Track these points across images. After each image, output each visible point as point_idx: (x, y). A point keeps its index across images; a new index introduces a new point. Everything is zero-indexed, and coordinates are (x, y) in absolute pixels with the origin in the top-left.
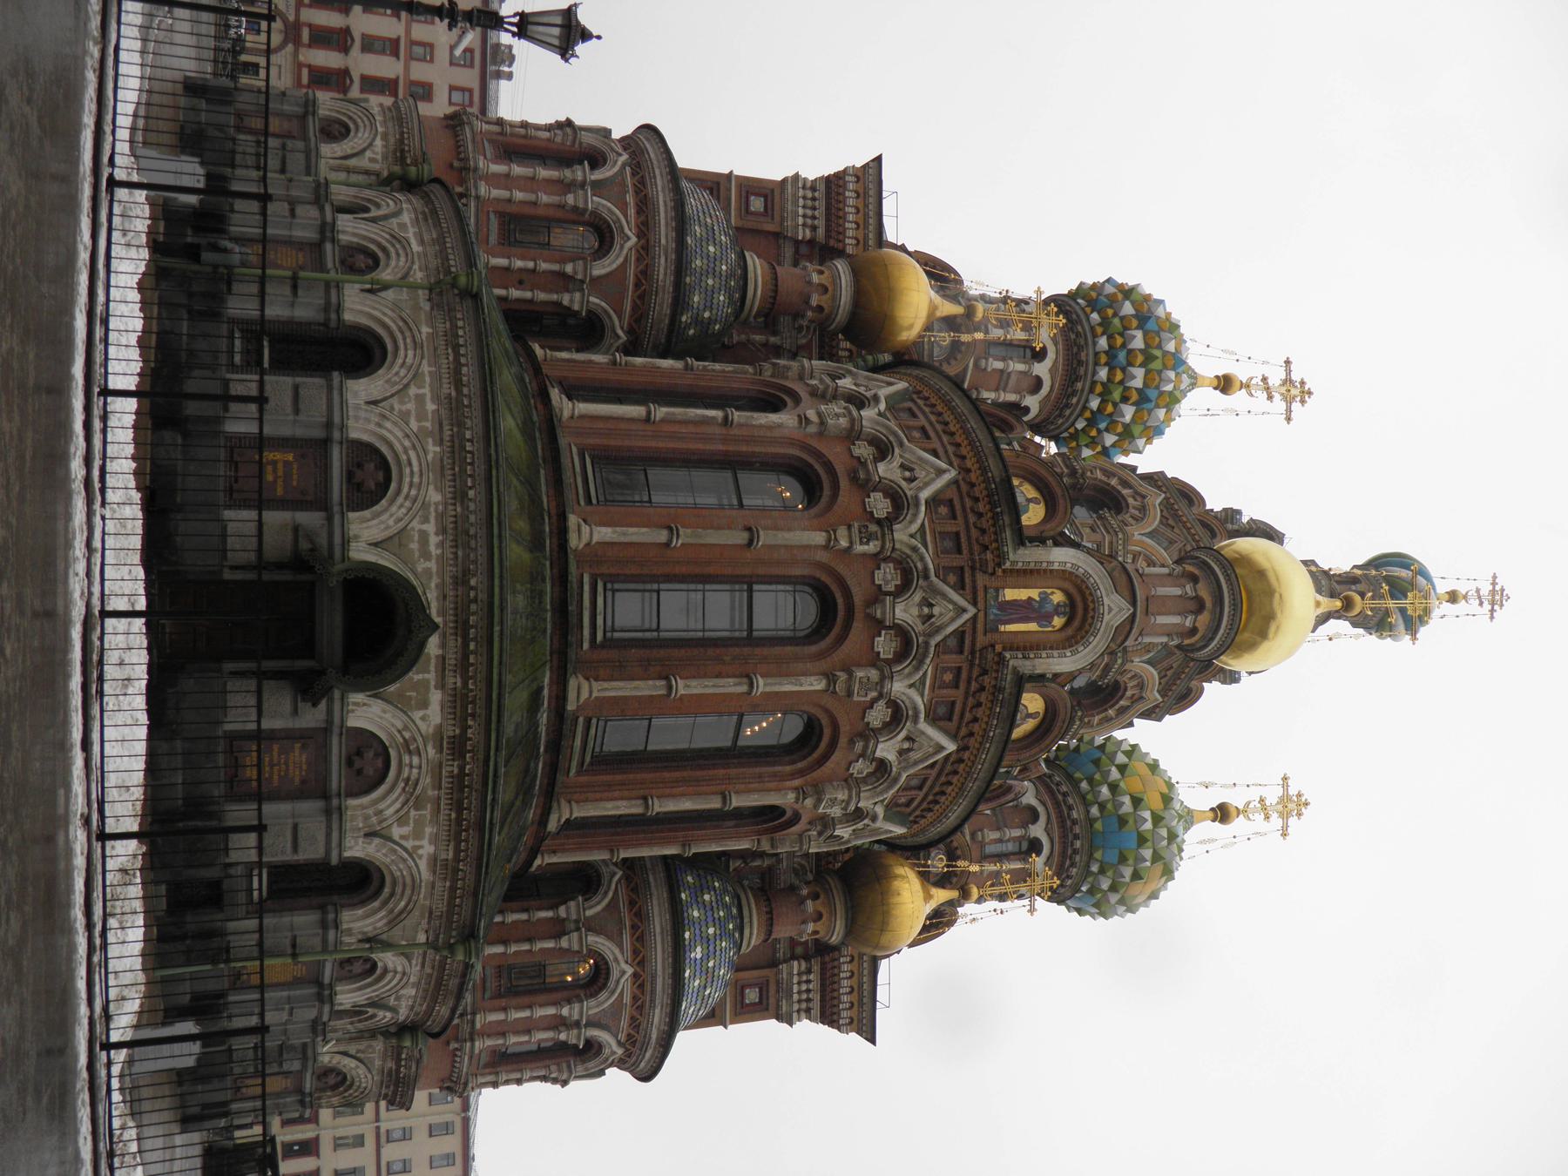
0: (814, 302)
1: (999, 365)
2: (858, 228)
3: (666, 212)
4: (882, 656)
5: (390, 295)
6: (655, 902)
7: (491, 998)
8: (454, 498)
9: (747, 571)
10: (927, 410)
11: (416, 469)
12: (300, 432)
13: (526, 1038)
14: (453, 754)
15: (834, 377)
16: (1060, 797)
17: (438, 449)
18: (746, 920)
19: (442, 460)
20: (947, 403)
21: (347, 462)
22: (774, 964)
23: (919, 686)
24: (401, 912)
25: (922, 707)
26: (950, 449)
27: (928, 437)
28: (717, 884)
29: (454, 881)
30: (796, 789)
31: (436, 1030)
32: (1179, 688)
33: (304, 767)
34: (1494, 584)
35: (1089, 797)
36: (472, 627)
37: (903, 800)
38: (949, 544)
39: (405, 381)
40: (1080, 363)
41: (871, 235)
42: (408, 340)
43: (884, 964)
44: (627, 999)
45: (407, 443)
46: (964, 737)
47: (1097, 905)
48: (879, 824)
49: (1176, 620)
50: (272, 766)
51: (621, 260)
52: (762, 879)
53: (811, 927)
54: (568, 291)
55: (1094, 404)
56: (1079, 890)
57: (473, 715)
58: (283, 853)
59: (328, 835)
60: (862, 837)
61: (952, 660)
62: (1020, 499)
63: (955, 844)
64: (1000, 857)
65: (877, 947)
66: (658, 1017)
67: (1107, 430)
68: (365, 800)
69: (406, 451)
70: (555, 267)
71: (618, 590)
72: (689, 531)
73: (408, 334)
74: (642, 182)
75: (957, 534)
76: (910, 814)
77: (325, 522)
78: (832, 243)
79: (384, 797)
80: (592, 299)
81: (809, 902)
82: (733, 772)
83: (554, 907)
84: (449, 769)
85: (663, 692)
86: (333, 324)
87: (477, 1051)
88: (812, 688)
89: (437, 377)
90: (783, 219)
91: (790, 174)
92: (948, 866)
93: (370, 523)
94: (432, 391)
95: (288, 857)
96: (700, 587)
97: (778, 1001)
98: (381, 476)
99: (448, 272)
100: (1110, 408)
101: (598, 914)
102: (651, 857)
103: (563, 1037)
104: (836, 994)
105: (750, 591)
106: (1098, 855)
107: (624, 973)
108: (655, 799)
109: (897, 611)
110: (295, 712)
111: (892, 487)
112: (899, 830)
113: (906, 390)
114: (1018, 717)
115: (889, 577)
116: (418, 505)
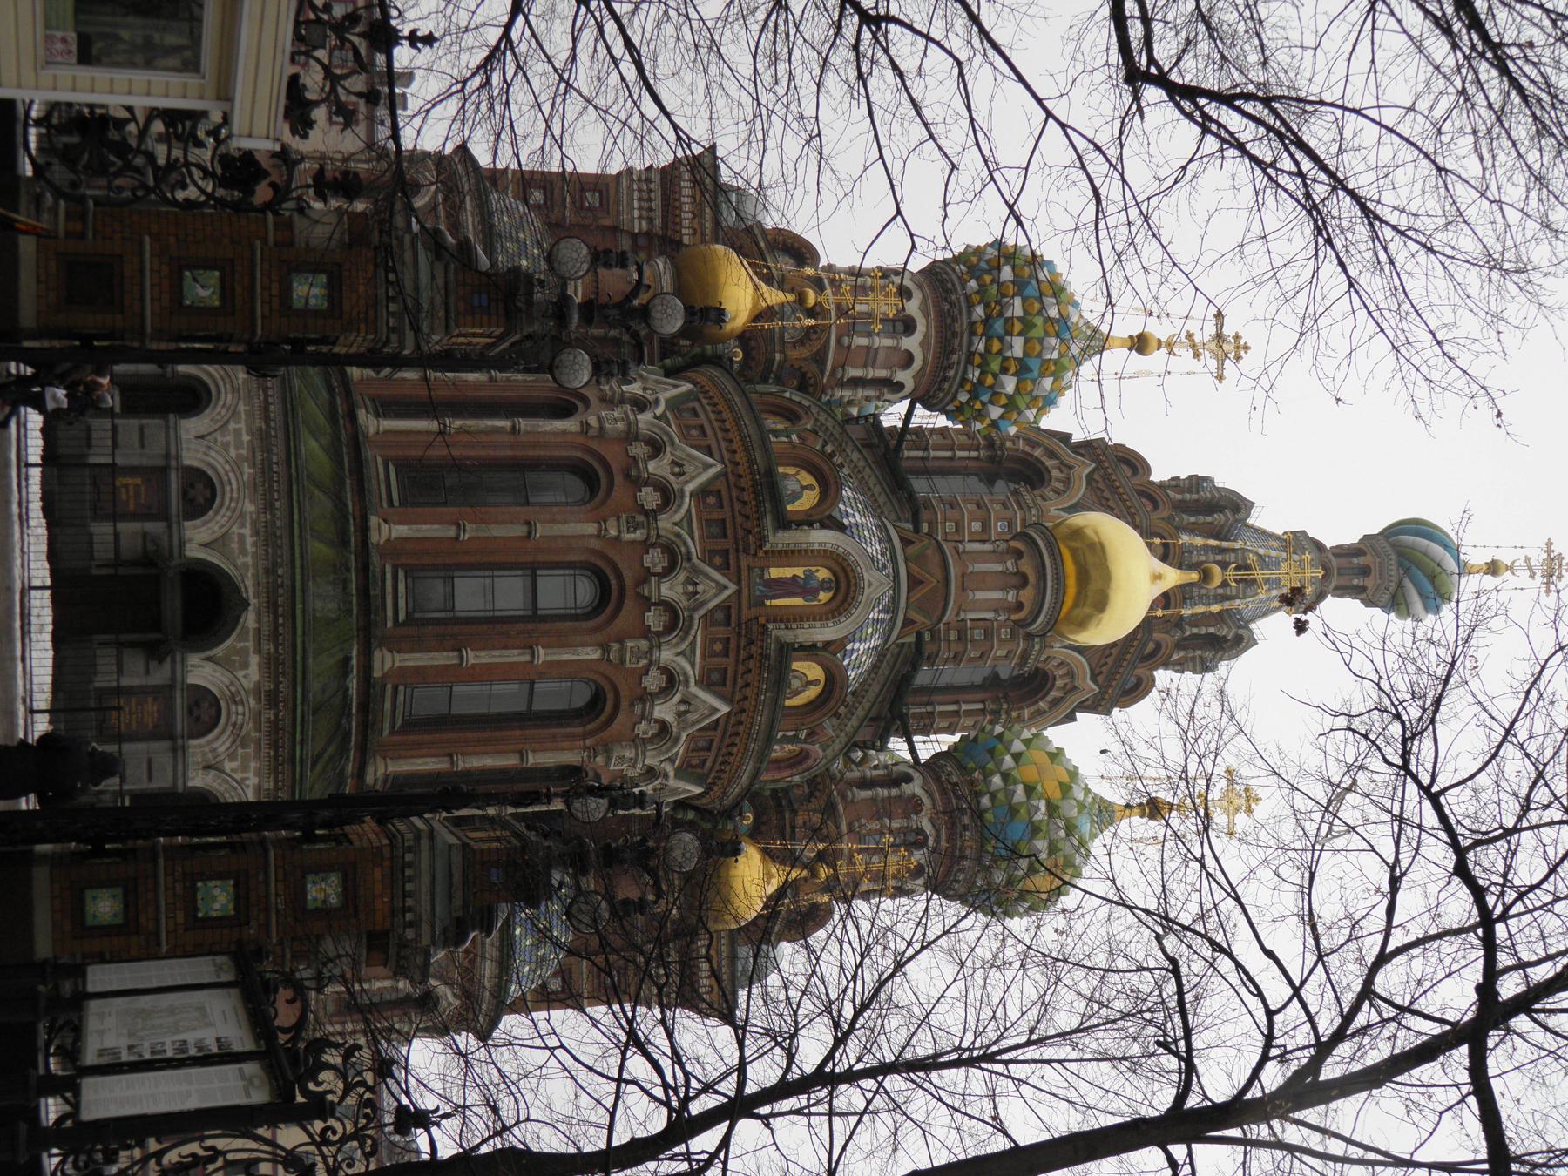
1: (863, 341)
9: (530, 559)
10: (709, 408)
11: (235, 486)
23: (688, 655)
34: (1549, 552)
37: (695, 762)
38: (715, 530)
40: (954, 334)
41: (708, 225)
55: (974, 374)
61: (721, 632)
67: (991, 402)
68: (203, 741)
75: (723, 521)
89: (250, 414)
100: (990, 380)
105: (534, 577)
113: (690, 392)
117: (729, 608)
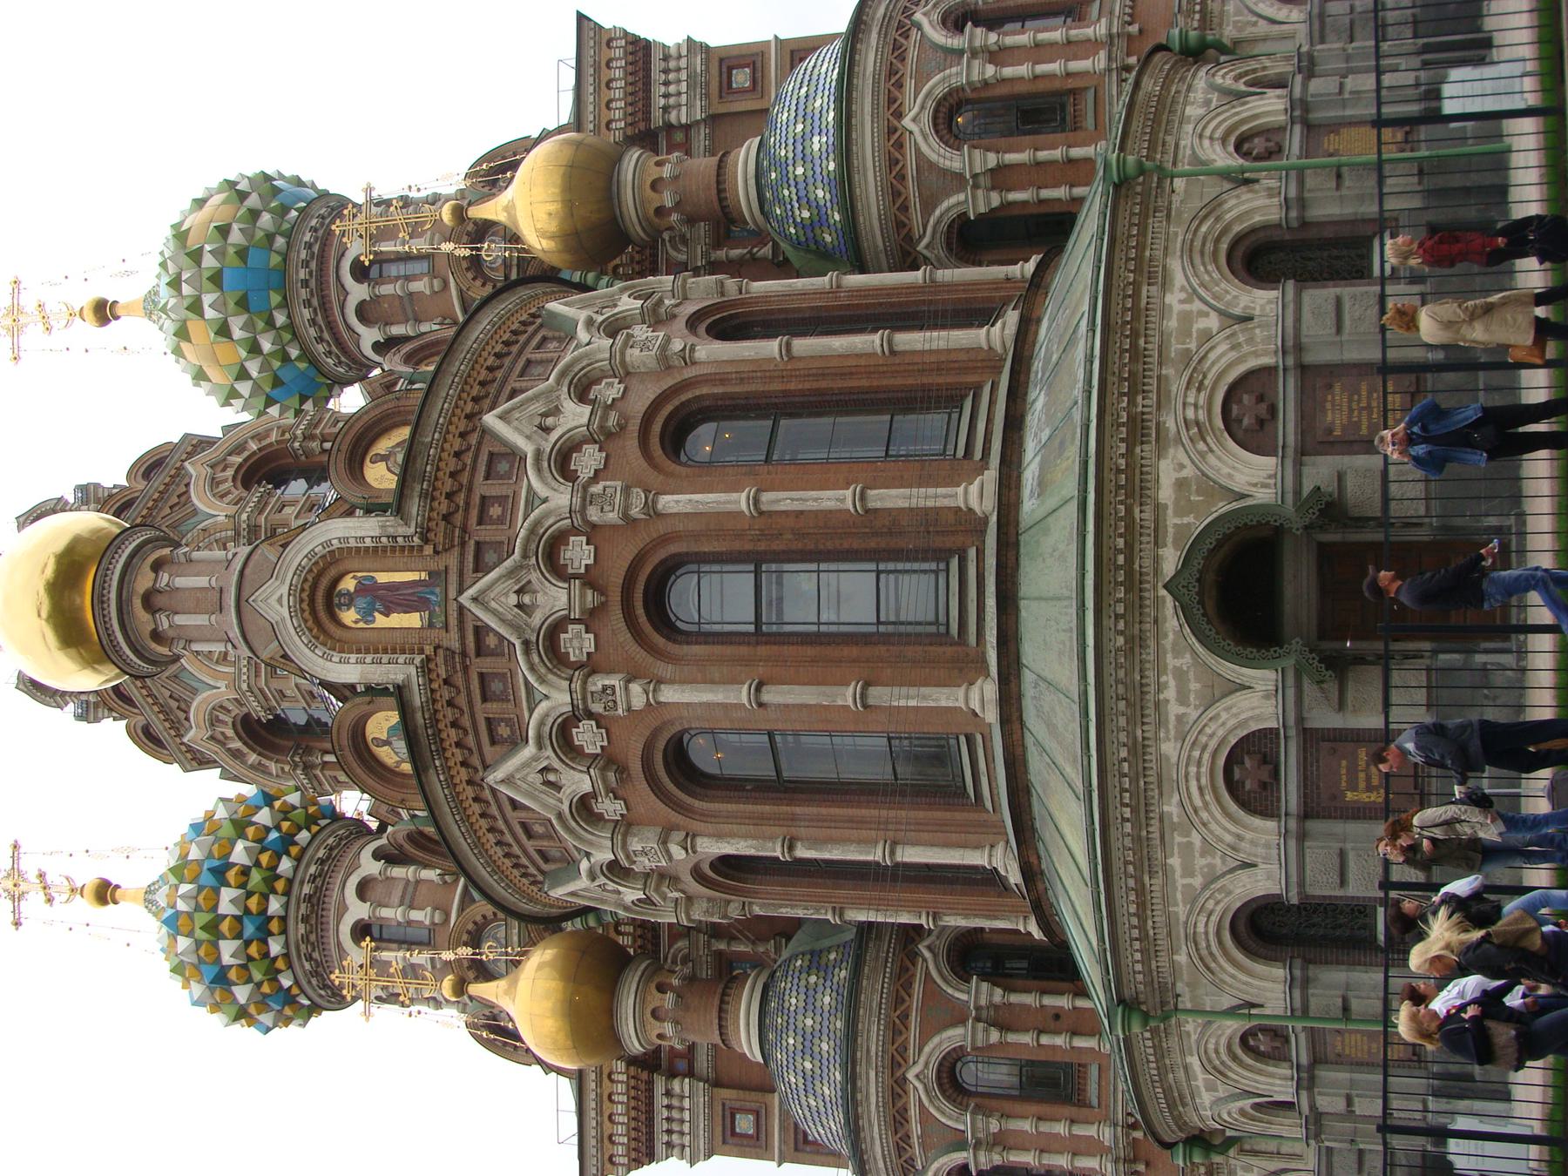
0: (669, 997)
1: (416, 915)
2: (610, 1096)
3: (869, 1112)
4: (584, 539)
5: (1227, 1002)
6: (874, 210)
7: (1086, 89)
8: (1144, 746)
9: (763, 650)
10: (524, 861)
11: (1193, 785)
12: (1338, 827)
13: (1042, 36)
14: (1143, 421)
15: (648, 901)
16: (326, 336)
17: (1166, 808)
18: (752, 182)
19: (1161, 794)
20: (496, 869)
21: (1278, 790)
22: (713, 119)
23: (533, 500)
24: (1205, 217)
25: (529, 473)
26: (494, 810)
27: (524, 826)
28: (793, 231)
29: (1139, 258)
30: (694, 363)
31: (1158, 57)
32: (160, 480)
33: (1329, 406)
35: (287, 336)
36: (1121, 584)
37: (555, 344)
38: (496, 686)
39: (1207, 893)
40: (305, 919)
41: (593, 1085)
42: (1203, 944)
43: (565, 117)
44: (909, 85)
45: (1205, 815)
46: (474, 430)
47: (277, 191)
48: (582, 316)
49: (180, 582)
50: (1369, 408)
51: (927, 1049)
52: (729, 231)
53: (666, 171)
54: (996, 1007)
55: (285, 865)
56: (301, 211)
57: (1119, 471)
58: (1354, 297)
59: (1298, 319)
60: (606, 296)
61: (485, 533)
62: (401, 745)
63: (470, 275)
64: (407, 258)
65: (578, 144)
66: (870, 58)
67: (268, 830)
68: (1252, 363)
69: (1206, 804)
70: (1012, 1038)
71: (930, 624)
72: (840, 703)
73: (1204, 952)
74: (900, 1150)
76: (541, 326)
77: (1306, 715)
78: (644, 1076)
79: (1230, 366)
80: (964, 997)
81: (669, 204)
82: (776, 386)
83: (1006, 205)
84: (1145, 402)
85: (871, 493)
86: (1298, 962)
87: (1103, 20)
88: (676, 497)
89: (1167, 900)
90: (711, 1106)
91: (700, 1165)
92: (479, 249)
93: (1250, 714)
94: (1174, 881)
95: (1347, 291)
96: (823, 628)
97: (707, 70)
98: (1237, 774)
99: (1154, 1032)
100: (265, 859)
101: (948, 196)
102: (881, 271)
103: (993, 37)
104: (630, 79)
105: (758, 622)
106: (275, 260)
107: (914, 120)
108: (879, 351)
109: (564, 599)
110: (1341, 477)
111: (571, 759)
112: (554, 306)
113: (552, 887)
114: (400, 458)
115: (576, 643)
116: (1190, 739)
117: (476, 570)
